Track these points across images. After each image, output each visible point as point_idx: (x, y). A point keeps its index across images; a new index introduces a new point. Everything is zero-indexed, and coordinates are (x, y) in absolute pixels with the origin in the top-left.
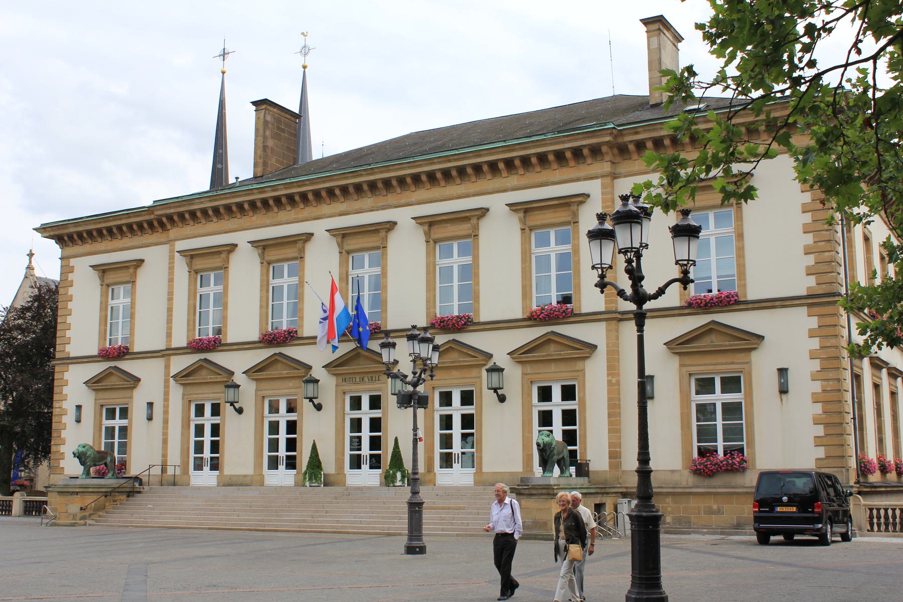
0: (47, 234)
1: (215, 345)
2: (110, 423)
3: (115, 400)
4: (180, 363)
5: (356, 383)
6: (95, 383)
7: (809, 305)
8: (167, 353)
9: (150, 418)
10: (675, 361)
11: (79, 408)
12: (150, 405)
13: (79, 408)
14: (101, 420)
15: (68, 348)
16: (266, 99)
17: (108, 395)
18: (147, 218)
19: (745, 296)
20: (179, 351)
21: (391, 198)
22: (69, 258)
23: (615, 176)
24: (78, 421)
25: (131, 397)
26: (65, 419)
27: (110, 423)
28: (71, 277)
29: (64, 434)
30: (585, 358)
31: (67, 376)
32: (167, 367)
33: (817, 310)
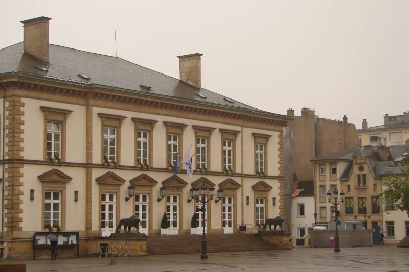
1: (149, 168)
2: (56, 201)
3: (54, 188)
4: (97, 173)
6: (42, 178)
7: (279, 179)
8: (88, 166)
9: (76, 200)
11: (32, 191)
12: (76, 193)
13: (32, 191)
15: (22, 154)
16: (43, 17)
17: (50, 185)
20: (97, 166)
22: (20, 96)
24: (32, 199)
25: (65, 188)
26: (21, 197)
27: (56, 201)
29: (21, 206)
31: (22, 171)
32: (88, 175)
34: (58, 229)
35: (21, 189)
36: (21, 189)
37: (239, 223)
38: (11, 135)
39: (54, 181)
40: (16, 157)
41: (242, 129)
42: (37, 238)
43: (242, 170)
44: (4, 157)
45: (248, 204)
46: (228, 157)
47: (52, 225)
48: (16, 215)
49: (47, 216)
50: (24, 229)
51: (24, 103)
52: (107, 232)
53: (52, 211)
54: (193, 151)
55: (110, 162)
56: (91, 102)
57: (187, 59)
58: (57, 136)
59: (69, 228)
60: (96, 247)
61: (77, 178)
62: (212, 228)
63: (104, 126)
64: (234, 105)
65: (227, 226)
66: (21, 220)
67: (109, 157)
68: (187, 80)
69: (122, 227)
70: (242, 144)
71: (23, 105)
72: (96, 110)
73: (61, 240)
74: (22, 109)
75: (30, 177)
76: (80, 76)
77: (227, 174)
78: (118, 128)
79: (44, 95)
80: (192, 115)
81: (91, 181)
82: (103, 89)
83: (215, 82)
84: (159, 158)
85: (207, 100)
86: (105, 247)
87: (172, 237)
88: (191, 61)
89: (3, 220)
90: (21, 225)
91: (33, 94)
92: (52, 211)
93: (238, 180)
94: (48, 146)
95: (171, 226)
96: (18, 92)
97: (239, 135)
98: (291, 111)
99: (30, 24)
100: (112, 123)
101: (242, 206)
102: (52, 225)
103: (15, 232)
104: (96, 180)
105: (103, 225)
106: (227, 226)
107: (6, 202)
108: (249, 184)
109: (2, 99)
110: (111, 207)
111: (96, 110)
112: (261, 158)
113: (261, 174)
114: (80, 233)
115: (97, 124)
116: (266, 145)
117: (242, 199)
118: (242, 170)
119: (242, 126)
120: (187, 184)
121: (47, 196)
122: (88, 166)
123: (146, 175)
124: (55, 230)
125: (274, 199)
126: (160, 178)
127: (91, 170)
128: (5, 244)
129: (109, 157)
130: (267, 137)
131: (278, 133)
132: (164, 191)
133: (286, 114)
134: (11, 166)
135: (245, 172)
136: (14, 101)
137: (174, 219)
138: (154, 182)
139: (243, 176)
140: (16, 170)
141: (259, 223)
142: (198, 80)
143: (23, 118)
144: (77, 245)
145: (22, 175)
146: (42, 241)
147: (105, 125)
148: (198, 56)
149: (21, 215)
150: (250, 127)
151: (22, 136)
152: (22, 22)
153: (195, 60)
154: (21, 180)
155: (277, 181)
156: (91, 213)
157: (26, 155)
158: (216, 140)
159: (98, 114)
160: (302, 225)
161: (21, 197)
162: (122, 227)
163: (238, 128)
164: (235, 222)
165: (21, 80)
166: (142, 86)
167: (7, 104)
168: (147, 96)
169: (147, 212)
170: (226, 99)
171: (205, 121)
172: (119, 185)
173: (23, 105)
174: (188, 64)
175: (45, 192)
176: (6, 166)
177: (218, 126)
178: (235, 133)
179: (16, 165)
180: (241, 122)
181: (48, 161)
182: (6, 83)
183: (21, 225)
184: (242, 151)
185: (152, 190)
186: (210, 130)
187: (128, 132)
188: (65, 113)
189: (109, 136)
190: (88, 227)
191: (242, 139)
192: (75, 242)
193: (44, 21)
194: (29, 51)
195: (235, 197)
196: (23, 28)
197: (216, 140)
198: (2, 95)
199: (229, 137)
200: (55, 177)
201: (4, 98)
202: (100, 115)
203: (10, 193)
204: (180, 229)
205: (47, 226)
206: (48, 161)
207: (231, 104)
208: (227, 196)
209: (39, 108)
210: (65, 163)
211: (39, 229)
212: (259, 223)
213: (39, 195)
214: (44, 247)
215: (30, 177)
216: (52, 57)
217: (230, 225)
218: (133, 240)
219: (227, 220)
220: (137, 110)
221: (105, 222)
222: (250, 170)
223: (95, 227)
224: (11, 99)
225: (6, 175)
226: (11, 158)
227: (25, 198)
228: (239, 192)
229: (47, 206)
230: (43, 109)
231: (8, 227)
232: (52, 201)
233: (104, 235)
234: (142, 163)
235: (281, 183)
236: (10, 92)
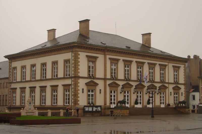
2: (92, 93)
4: (109, 82)
6: (87, 84)
8: (105, 79)
9: (100, 93)
11: (83, 89)
12: (100, 90)
13: (83, 89)
14: (65, 93)
15: (79, 74)
19: (166, 81)
20: (109, 79)
24: (83, 92)
25: (96, 88)
26: (79, 92)
27: (92, 93)
29: (79, 95)
31: (79, 81)
33: (185, 86)
34: (93, 104)
35: (79, 88)
36: (79, 88)
37: (167, 103)
38: (75, 67)
39: (91, 85)
40: (77, 76)
41: (168, 64)
42: (85, 108)
43: (168, 81)
44: (72, 75)
45: (171, 95)
46: (162, 76)
47: (91, 103)
48: (77, 99)
49: (89, 99)
50: (80, 104)
51: (79, 54)
52: (113, 106)
53: (91, 97)
54: (148, 73)
55: (114, 77)
56: (106, 53)
57: (145, 35)
58: (93, 67)
59: (97, 104)
60: (108, 112)
61: (101, 84)
62: (156, 104)
63: (111, 63)
64: (165, 54)
65: (162, 104)
66: (79, 101)
67: (113, 76)
68: (145, 44)
69: (119, 104)
70: (168, 70)
71: (79, 55)
72: (108, 57)
73: (95, 109)
74: (79, 56)
75: (82, 84)
76: (101, 43)
77: (162, 83)
78: (117, 64)
79: (87, 51)
80: (148, 58)
81: (106, 85)
82: (111, 48)
83: (157, 44)
84: (134, 76)
85: (154, 52)
86: (112, 112)
87: (139, 108)
88: (147, 36)
89: (72, 101)
90: (79, 103)
91: (83, 50)
92: (91, 97)
93: (167, 85)
94: (89, 71)
95: (139, 104)
96: (77, 50)
97: (167, 67)
98: (189, 56)
99: (82, 22)
100: (115, 62)
101: (169, 96)
102: (91, 103)
103: (76, 105)
104: (109, 85)
105: (111, 103)
106: (162, 104)
107: (73, 93)
108: (171, 87)
109: (71, 53)
110: (114, 96)
111: (108, 57)
112: (176, 76)
113: (176, 82)
114: (102, 106)
115: (108, 62)
116: (178, 70)
117: (169, 93)
118: (168, 81)
119: (168, 63)
120: (145, 86)
121: (89, 91)
122: (105, 79)
123: (128, 83)
124: (92, 105)
125: (182, 93)
126: (134, 84)
128: (73, 110)
129: (113, 76)
130: (179, 67)
131: (184, 66)
132: (136, 90)
133: (187, 57)
134: (75, 79)
135: (170, 82)
136: (76, 53)
137: (140, 101)
138: (132, 86)
139: (168, 83)
140: (77, 81)
141: (176, 103)
142: (150, 44)
143: (79, 60)
144: (101, 111)
145: (79, 83)
146: (87, 109)
147: (112, 63)
148: (150, 34)
149: (79, 99)
150: (172, 63)
151: (79, 67)
152: (79, 22)
153: (148, 36)
154: (79, 84)
155: (183, 85)
156: (106, 98)
157: (81, 75)
158: (157, 69)
159: (109, 58)
160: (194, 104)
161: (79, 92)
162: (119, 104)
163: (167, 64)
164: (165, 103)
165: (79, 45)
166: (126, 47)
167: (73, 54)
168: (129, 51)
169: (129, 98)
170: (161, 52)
172: (118, 87)
173: (79, 55)
174: (145, 37)
175: (88, 90)
176: (73, 79)
177: (158, 63)
179: (76, 79)
180: (168, 61)
181: (89, 77)
182: (73, 46)
183: (79, 103)
184: (168, 73)
185: (131, 89)
186: (155, 64)
187: (121, 65)
188: (96, 58)
189: (113, 67)
190: (105, 104)
191: (168, 68)
192: (100, 110)
193: (87, 21)
194: (81, 33)
195: (165, 92)
196: (79, 24)
197: (157, 69)
198: (71, 51)
199: (163, 67)
200: (92, 84)
201: (72, 52)
202: (110, 59)
203: (75, 90)
204: (142, 105)
205: (89, 103)
206: (89, 77)
207: (164, 54)
208: (162, 92)
209: (85, 56)
210: (96, 78)
211: (86, 104)
212: (176, 103)
213: (85, 91)
214: (88, 112)
215: (82, 84)
216: (90, 35)
217: (163, 104)
218: (123, 109)
219: (162, 101)
220: (125, 56)
221: (112, 102)
222: (172, 81)
223: (108, 104)
224: (75, 52)
225: (73, 83)
226: (75, 76)
227: (80, 92)
228: (167, 90)
229: (89, 95)
230: (87, 56)
231: (74, 103)
232: (91, 93)
233: (111, 107)
234: (127, 78)
235: (185, 86)
236: (74, 50)
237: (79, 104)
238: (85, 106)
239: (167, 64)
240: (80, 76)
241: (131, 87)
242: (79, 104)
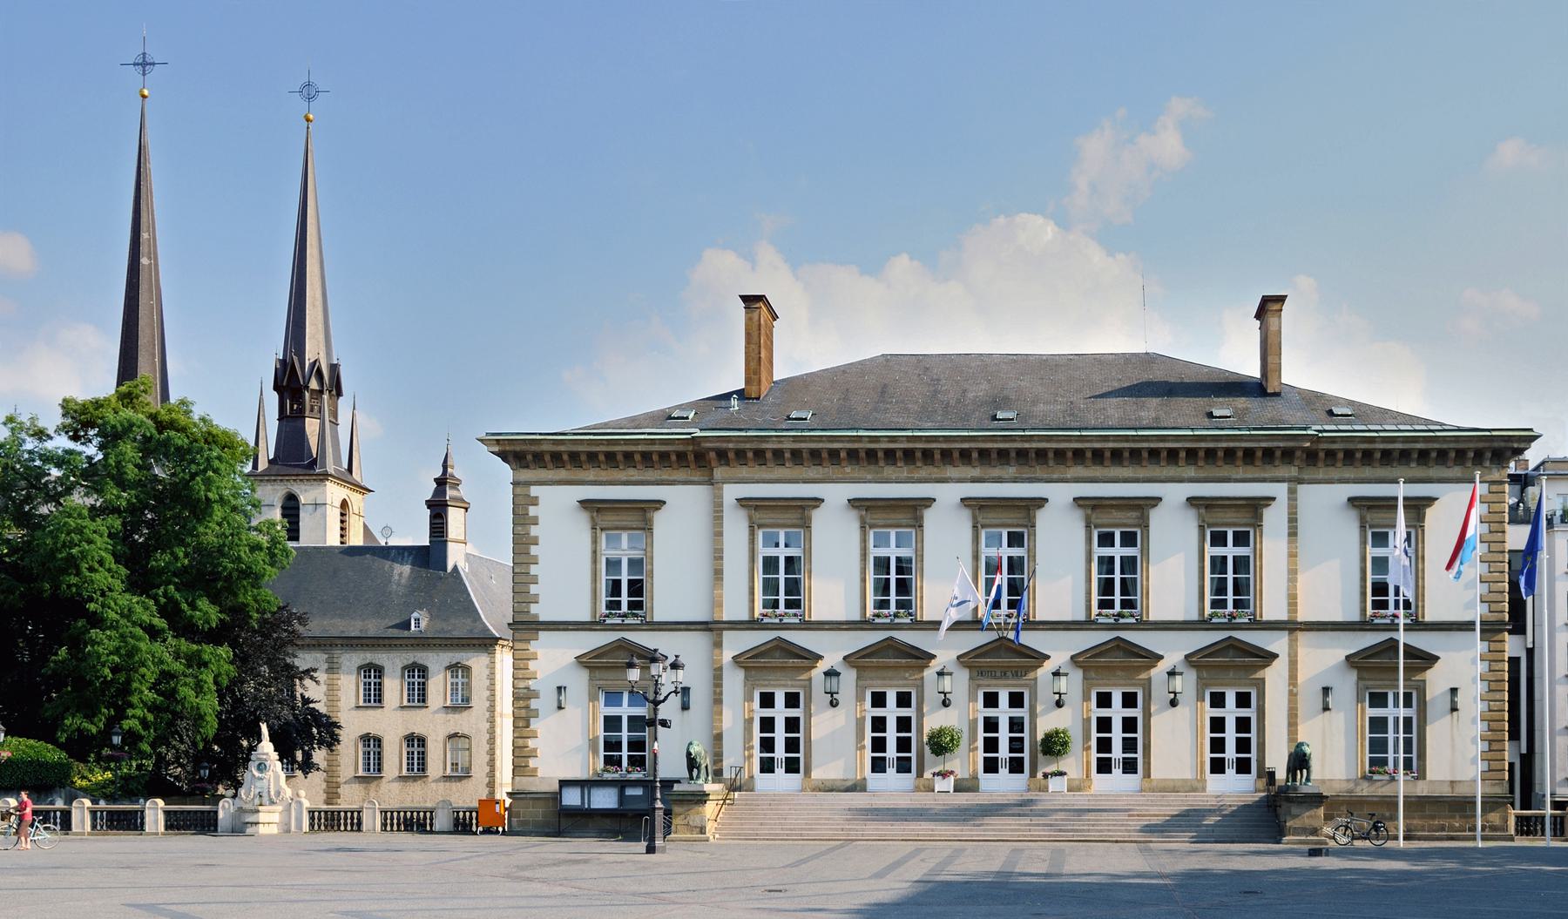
0: (496, 449)
4: (736, 643)
5: (995, 678)
8: (712, 628)
10: (1353, 676)
15: (534, 609)
18: (681, 448)
21: (1039, 471)
22: (529, 484)
23: (1301, 481)
28: (532, 511)
30: (1265, 666)
32: (718, 645)
72: (731, 492)
91: (563, 474)
127: (721, 636)
150: (1347, 481)
157: (543, 611)
171: (1137, 481)
178: (1256, 506)
180: (1293, 471)
202: (743, 502)
237: (535, 770)
238: (564, 783)
239: (1279, 490)
240: (541, 619)
241: (923, 668)
242: (535, 770)
